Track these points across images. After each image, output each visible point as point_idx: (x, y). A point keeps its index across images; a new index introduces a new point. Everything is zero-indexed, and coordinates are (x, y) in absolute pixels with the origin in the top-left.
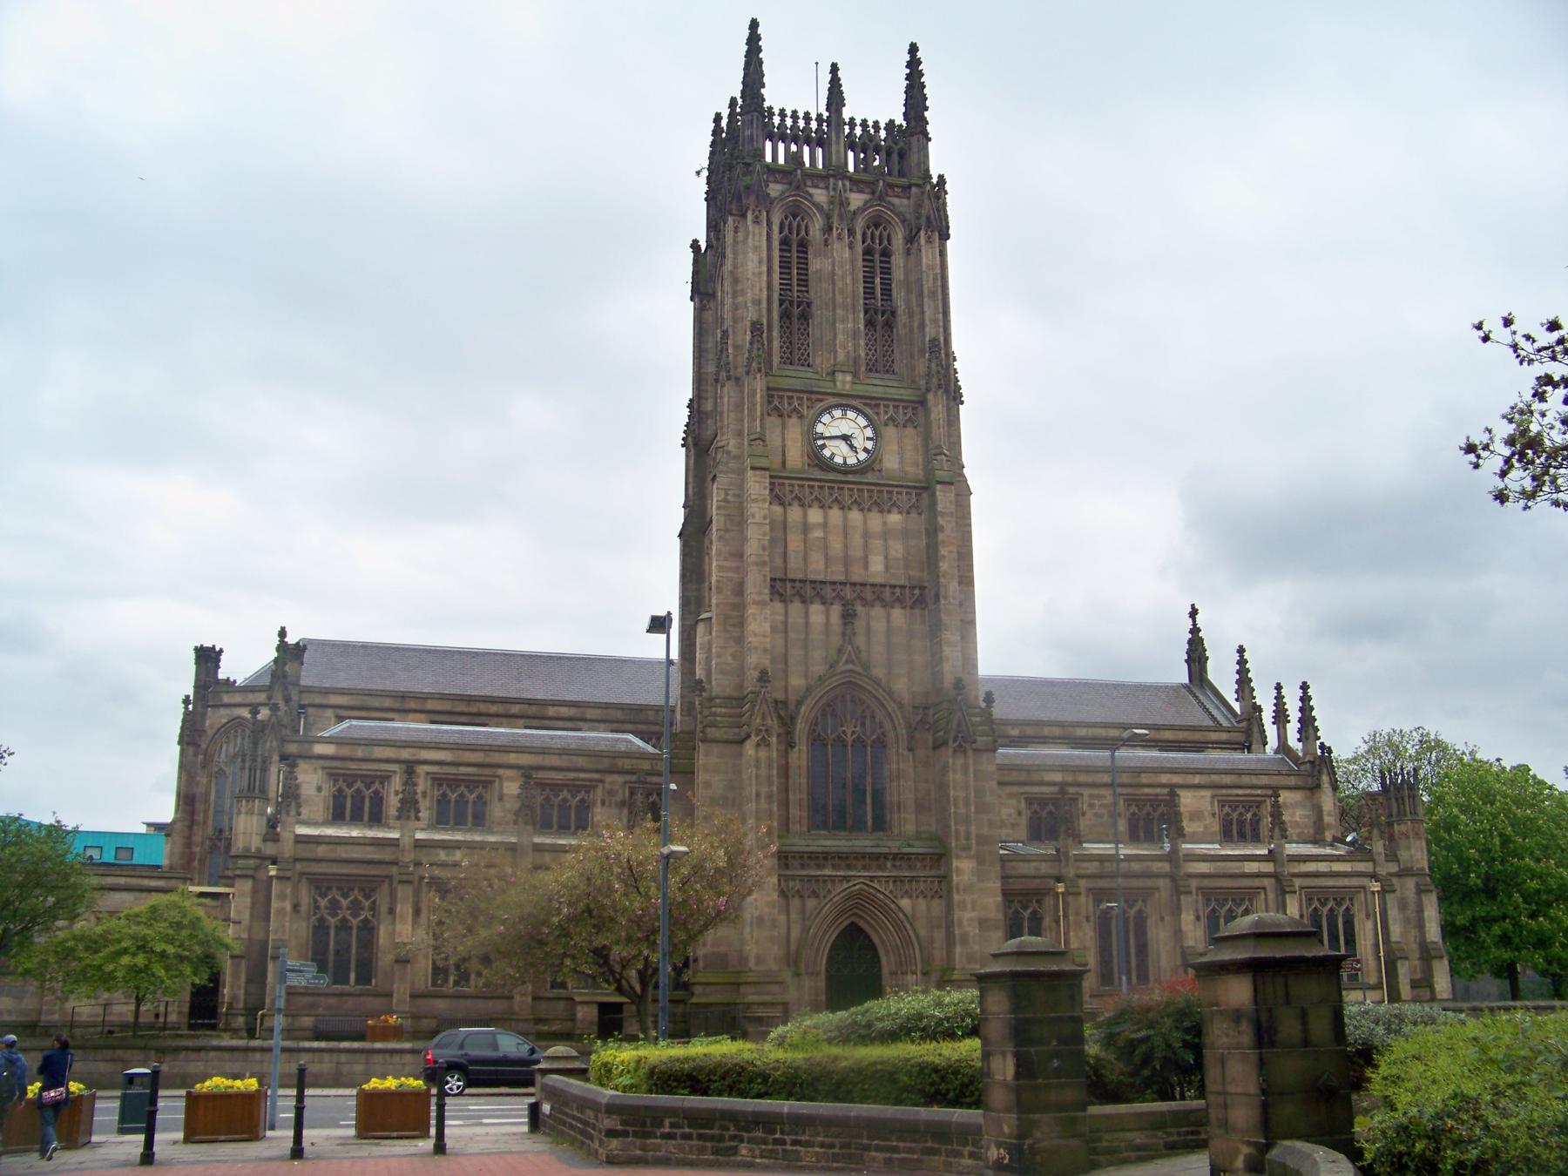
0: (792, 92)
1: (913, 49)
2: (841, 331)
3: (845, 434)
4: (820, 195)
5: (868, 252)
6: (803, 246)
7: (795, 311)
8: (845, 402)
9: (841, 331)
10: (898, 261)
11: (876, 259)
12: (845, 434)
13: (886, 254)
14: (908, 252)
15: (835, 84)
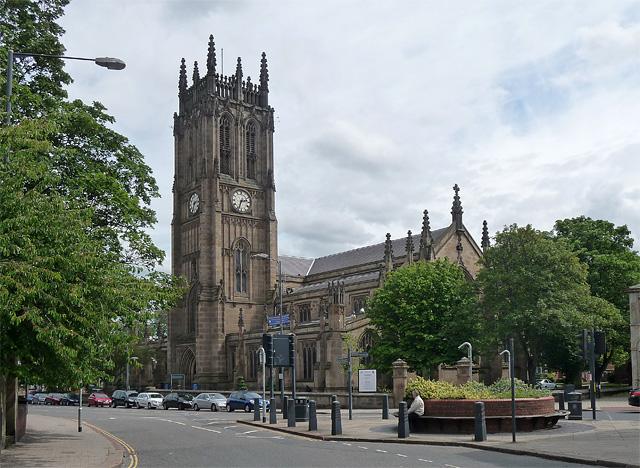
0: (225, 69)
1: (264, 55)
2: (239, 162)
3: (240, 200)
4: (234, 111)
5: (248, 134)
6: (227, 129)
7: (226, 155)
8: (241, 189)
9: (239, 162)
10: (258, 138)
11: (250, 135)
12: (240, 200)
13: (253, 135)
14: (261, 136)
15: (239, 67)
